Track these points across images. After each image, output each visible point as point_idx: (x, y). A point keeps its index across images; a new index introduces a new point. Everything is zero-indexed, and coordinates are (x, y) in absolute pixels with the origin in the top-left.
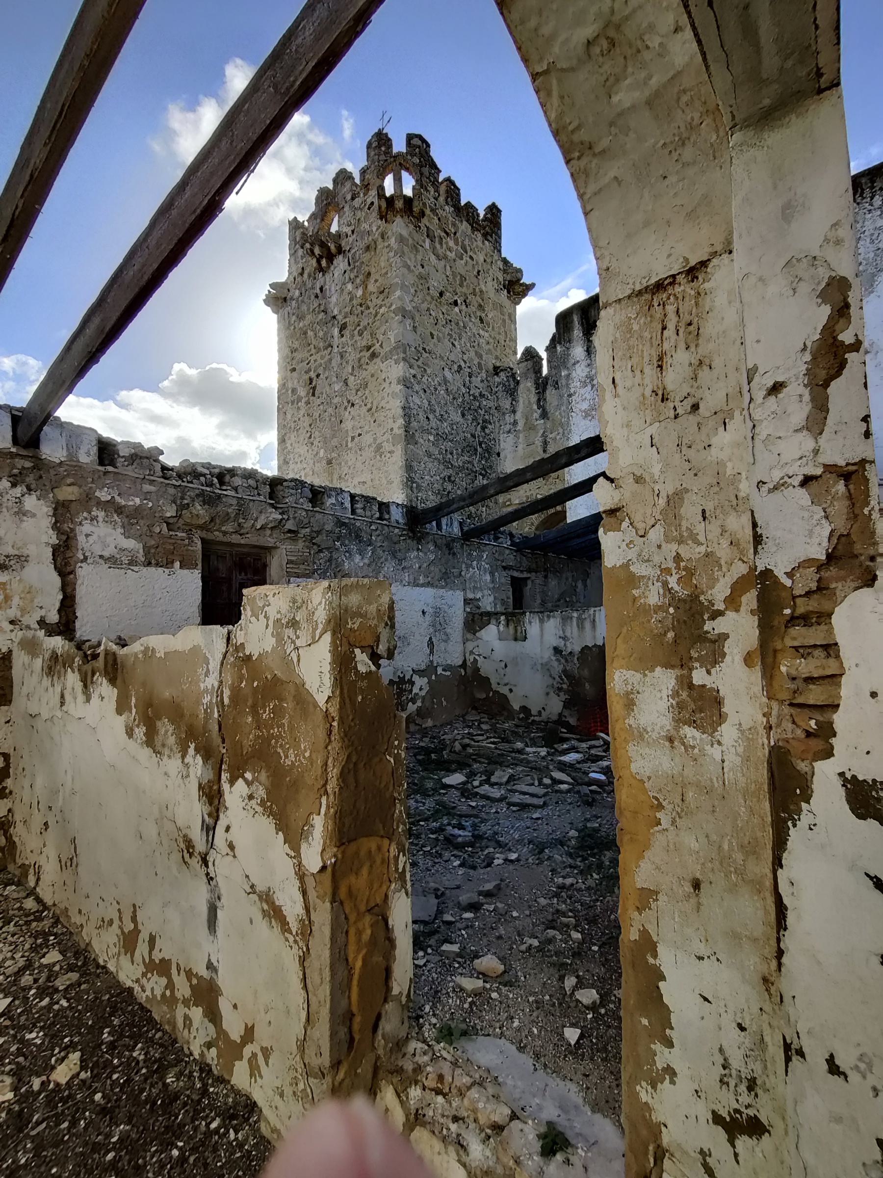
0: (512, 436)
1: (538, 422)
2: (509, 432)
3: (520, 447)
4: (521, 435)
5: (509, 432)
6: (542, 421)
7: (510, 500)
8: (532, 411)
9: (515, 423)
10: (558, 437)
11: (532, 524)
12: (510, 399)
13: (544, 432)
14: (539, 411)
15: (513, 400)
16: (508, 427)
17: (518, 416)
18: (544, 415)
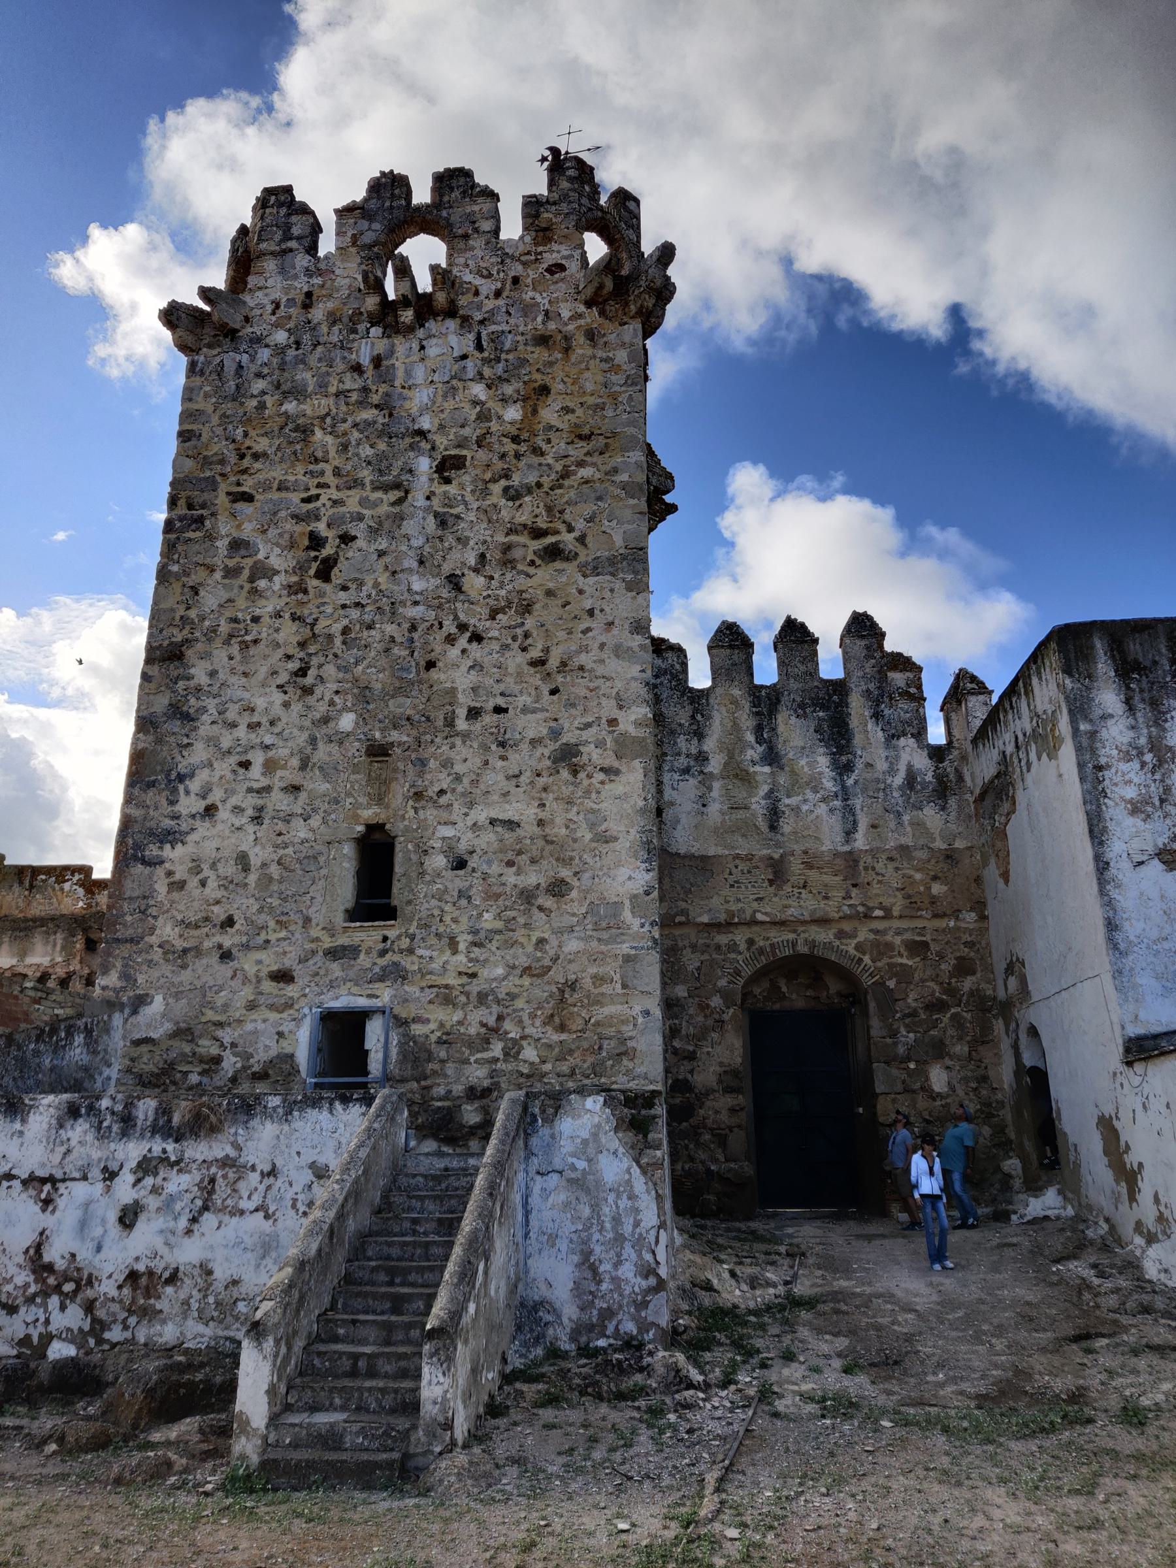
0: (692, 782)
1: (758, 768)
2: (686, 771)
3: (714, 808)
4: (717, 785)
5: (686, 771)
6: (767, 769)
7: (685, 912)
8: (746, 746)
9: (702, 758)
10: (805, 808)
11: (738, 973)
12: (689, 709)
13: (771, 791)
14: (760, 749)
15: (696, 711)
16: (683, 762)
17: (710, 745)
18: (772, 757)
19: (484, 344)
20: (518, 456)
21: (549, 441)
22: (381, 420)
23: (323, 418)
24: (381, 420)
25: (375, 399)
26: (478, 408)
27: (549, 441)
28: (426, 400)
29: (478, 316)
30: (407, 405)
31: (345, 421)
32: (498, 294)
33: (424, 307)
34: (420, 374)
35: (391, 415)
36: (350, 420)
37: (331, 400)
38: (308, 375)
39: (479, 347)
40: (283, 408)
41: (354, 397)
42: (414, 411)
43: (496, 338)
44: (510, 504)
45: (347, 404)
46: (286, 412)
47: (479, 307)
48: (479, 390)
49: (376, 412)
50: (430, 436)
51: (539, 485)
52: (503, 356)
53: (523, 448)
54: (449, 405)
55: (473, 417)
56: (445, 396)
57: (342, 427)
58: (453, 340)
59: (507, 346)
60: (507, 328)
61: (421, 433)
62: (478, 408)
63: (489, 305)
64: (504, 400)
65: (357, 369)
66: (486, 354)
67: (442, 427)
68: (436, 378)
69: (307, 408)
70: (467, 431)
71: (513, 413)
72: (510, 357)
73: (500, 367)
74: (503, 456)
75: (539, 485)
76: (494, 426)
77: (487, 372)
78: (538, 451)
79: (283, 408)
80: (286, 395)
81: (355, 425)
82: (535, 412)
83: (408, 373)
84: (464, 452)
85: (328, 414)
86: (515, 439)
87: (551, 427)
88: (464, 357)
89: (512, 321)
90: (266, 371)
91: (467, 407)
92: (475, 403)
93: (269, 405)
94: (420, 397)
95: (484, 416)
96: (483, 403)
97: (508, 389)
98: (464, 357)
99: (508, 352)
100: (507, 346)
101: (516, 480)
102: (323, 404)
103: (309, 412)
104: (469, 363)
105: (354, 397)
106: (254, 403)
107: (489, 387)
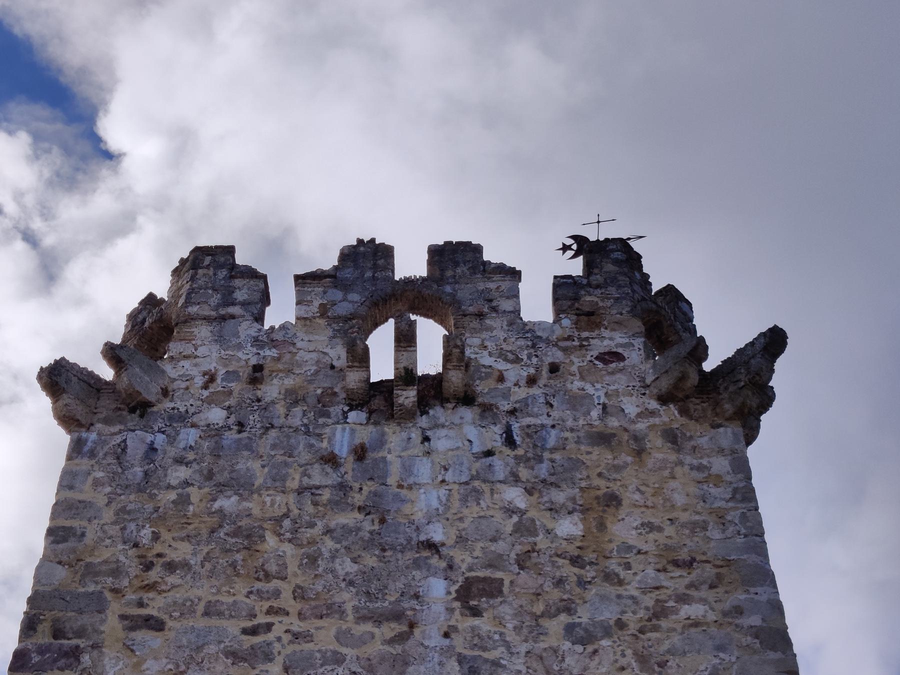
19: (518, 440)
20: (582, 583)
21: (628, 566)
22: (367, 526)
23: (278, 521)
24: (367, 526)
25: (358, 499)
26: (515, 519)
27: (628, 566)
28: (435, 504)
29: (505, 406)
30: (407, 509)
31: (312, 525)
32: (532, 381)
33: (432, 391)
34: (424, 470)
35: (382, 521)
36: (320, 524)
37: (292, 498)
38: (256, 465)
39: (510, 441)
40: (217, 505)
41: (326, 495)
42: (419, 517)
43: (531, 432)
44: (579, 648)
45: (315, 504)
46: (221, 510)
47: (506, 395)
48: (515, 495)
49: (360, 516)
50: (444, 551)
51: (621, 625)
52: (546, 455)
53: (589, 573)
54: (472, 511)
55: (509, 529)
56: (464, 500)
57: (307, 534)
58: (471, 432)
59: (551, 442)
60: (549, 422)
61: (432, 546)
62: (515, 519)
63: (521, 393)
64: (553, 510)
65: (331, 460)
66: (520, 452)
67: (462, 540)
68: (449, 476)
69: (252, 504)
70: (501, 547)
71: (569, 527)
72: (557, 456)
73: (543, 470)
74: (560, 582)
75: (621, 625)
76: (541, 541)
77: (524, 473)
78: (610, 578)
79: (217, 505)
80: (221, 488)
81: (328, 531)
82: (602, 526)
83: (407, 469)
84: (499, 575)
85: (286, 516)
86: (575, 561)
87: (629, 548)
88: (489, 453)
89: (555, 414)
90: (191, 456)
91: (499, 516)
92: (510, 511)
93: (194, 499)
94: (426, 501)
95: (526, 528)
96: (522, 513)
97: (559, 497)
98: (489, 453)
99: (553, 450)
100: (551, 442)
101: (584, 616)
102: (278, 502)
103: (256, 512)
104: (496, 461)
105: (326, 495)
106: (172, 496)
107: (529, 492)
